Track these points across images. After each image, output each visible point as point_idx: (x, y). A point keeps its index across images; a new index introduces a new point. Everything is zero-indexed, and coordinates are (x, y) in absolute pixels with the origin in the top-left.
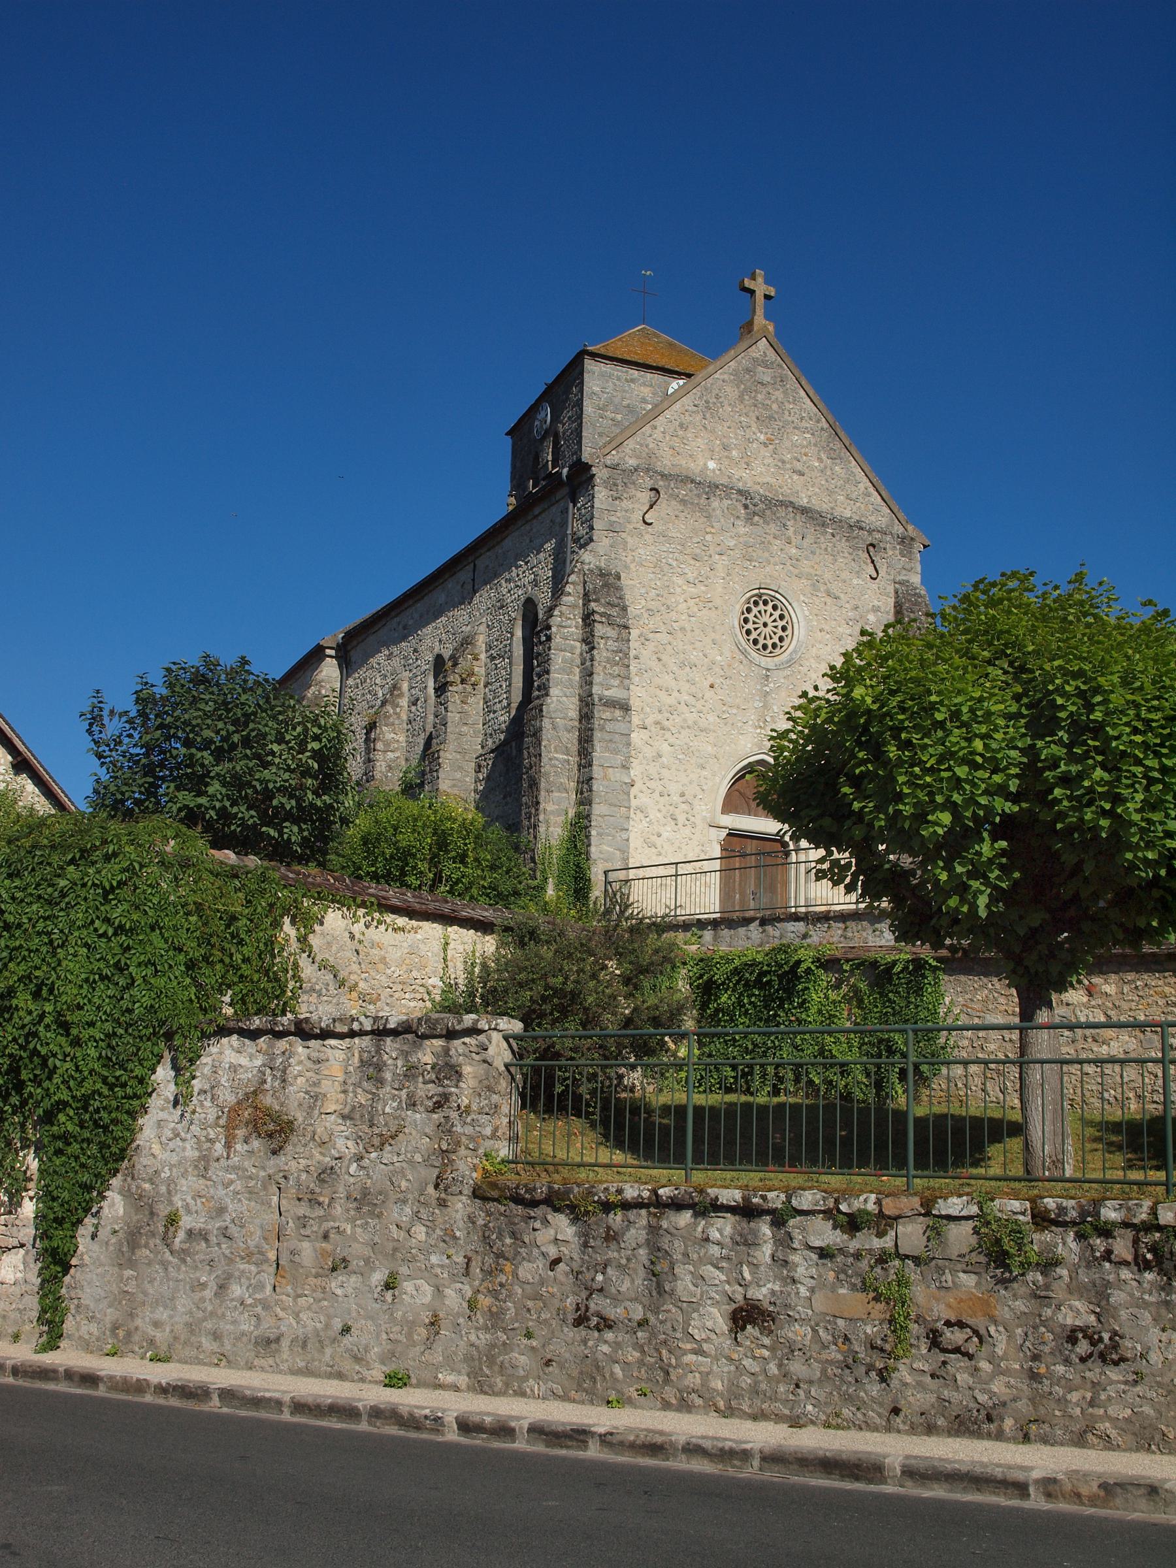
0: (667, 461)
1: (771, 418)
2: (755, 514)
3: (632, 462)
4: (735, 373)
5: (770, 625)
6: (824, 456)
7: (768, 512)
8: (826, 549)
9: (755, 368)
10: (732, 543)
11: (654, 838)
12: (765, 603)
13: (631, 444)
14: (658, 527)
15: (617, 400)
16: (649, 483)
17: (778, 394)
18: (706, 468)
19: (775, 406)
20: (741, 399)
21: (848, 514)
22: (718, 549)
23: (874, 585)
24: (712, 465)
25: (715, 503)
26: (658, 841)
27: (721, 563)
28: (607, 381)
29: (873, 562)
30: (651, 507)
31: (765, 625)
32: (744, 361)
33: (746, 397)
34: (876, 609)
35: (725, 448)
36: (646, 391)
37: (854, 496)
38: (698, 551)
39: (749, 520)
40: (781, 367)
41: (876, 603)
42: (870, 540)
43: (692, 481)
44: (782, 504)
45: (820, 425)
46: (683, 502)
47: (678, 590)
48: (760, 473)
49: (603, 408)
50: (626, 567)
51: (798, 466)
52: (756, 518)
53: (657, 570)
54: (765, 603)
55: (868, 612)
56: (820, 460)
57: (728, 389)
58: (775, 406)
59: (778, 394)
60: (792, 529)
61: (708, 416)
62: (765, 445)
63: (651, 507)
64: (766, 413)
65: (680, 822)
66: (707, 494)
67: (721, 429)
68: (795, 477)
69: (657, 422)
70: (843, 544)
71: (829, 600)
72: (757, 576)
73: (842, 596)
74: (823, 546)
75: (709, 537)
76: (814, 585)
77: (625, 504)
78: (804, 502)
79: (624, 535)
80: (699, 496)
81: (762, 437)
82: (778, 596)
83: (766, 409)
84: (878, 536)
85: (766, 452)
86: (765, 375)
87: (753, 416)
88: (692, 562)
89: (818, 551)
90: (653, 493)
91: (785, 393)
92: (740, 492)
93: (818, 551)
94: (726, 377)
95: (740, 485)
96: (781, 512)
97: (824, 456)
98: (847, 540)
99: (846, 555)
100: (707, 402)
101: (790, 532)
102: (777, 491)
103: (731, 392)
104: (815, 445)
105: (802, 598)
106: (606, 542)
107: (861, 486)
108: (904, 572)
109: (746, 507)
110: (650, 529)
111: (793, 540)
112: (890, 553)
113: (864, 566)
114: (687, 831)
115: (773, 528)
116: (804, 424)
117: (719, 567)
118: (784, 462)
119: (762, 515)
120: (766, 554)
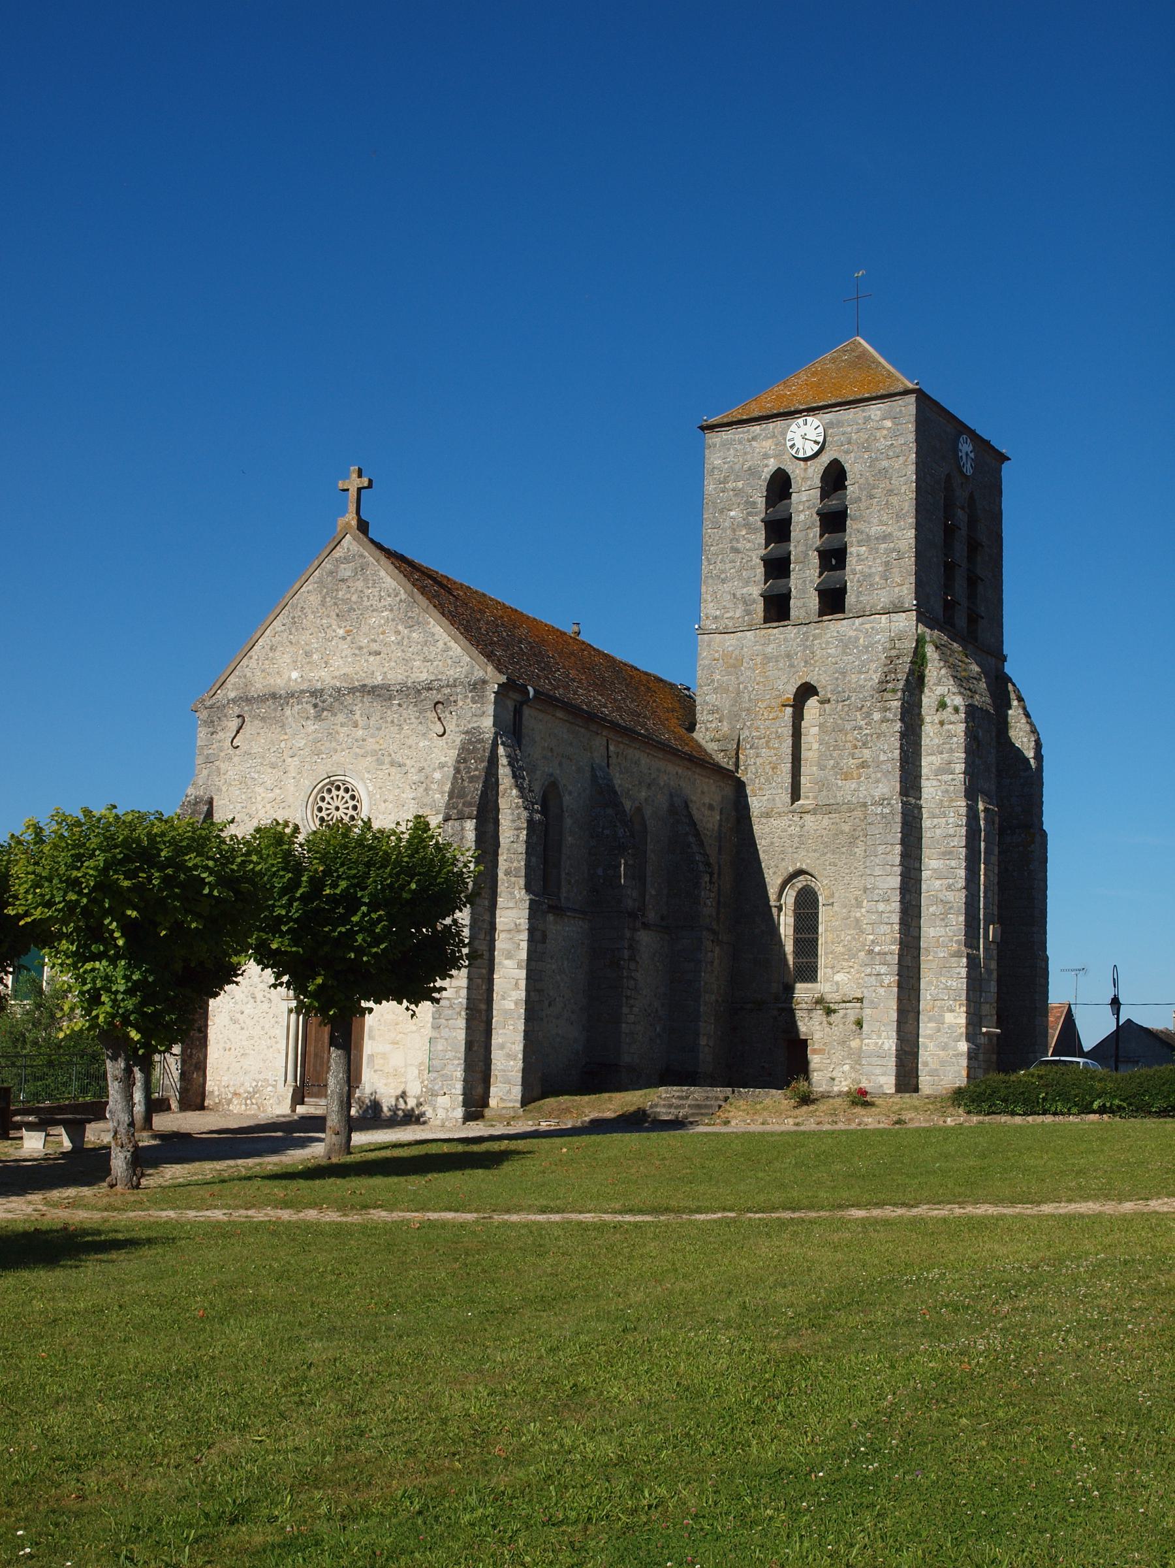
0: (259, 685)
1: (352, 609)
2: (324, 710)
3: (232, 695)
4: (320, 582)
5: (332, 807)
6: (400, 627)
7: (336, 704)
8: (392, 722)
9: (338, 567)
10: (302, 743)
11: (238, 1016)
12: (338, 788)
13: (232, 679)
14: (243, 748)
15: (737, 467)
16: (237, 711)
17: (360, 584)
18: (290, 678)
19: (354, 598)
20: (323, 603)
21: (424, 676)
22: (290, 753)
23: (441, 742)
24: (295, 675)
25: (288, 712)
26: (241, 1018)
27: (293, 764)
28: (729, 449)
29: (439, 719)
30: (238, 732)
31: (337, 809)
32: (327, 565)
33: (328, 599)
34: (442, 766)
35: (308, 654)
36: (768, 445)
37: (431, 657)
38: (273, 760)
39: (318, 717)
40: (362, 556)
41: (443, 759)
42: (439, 697)
43: (274, 696)
44: (352, 690)
45: (398, 599)
46: (263, 719)
47: (259, 798)
48: (338, 665)
49: (725, 481)
50: (219, 790)
51: (375, 647)
52: (325, 713)
53: (243, 785)
54: (338, 788)
55: (434, 770)
56: (398, 632)
57: (311, 598)
58: (354, 598)
59: (360, 584)
60: (358, 713)
61: (293, 630)
62: (344, 638)
63: (238, 732)
64: (345, 608)
65: (258, 1000)
66: (281, 705)
67: (305, 637)
68: (371, 658)
69: (252, 653)
70: (411, 712)
71: (393, 770)
72: (322, 770)
73: (408, 762)
74: (389, 720)
75: (283, 745)
76: (377, 760)
77: (221, 735)
78: (379, 680)
79: (217, 763)
80: (275, 710)
81: (341, 632)
82: (347, 779)
83: (347, 603)
84: (447, 691)
85: (344, 645)
86: (346, 571)
87: (333, 615)
88: (270, 770)
89: (384, 725)
90: (240, 720)
91: (366, 580)
92: (314, 693)
93: (384, 725)
94: (310, 587)
95: (319, 686)
96: (349, 699)
97: (400, 627)
98: (416, 705)
99: (413, 720)
100: (293, 618)
101: (357, 717)
102: (352, 679)
103: (314, 599)
104: (393, 620)
105: (367, 775)
106: (205, 772)
107: (440, 644)
108: (475, 719)
109: (315, 706)
110: (237, 752)
111: (360, 722)
112: (460, 703)
113: (432, 726)
114: (265, 1006)
115: (341, 718)
116: (383, 603)
117: (291, 769)
118: (360, 648)
119: (330, 709)
120: (334, 744)
